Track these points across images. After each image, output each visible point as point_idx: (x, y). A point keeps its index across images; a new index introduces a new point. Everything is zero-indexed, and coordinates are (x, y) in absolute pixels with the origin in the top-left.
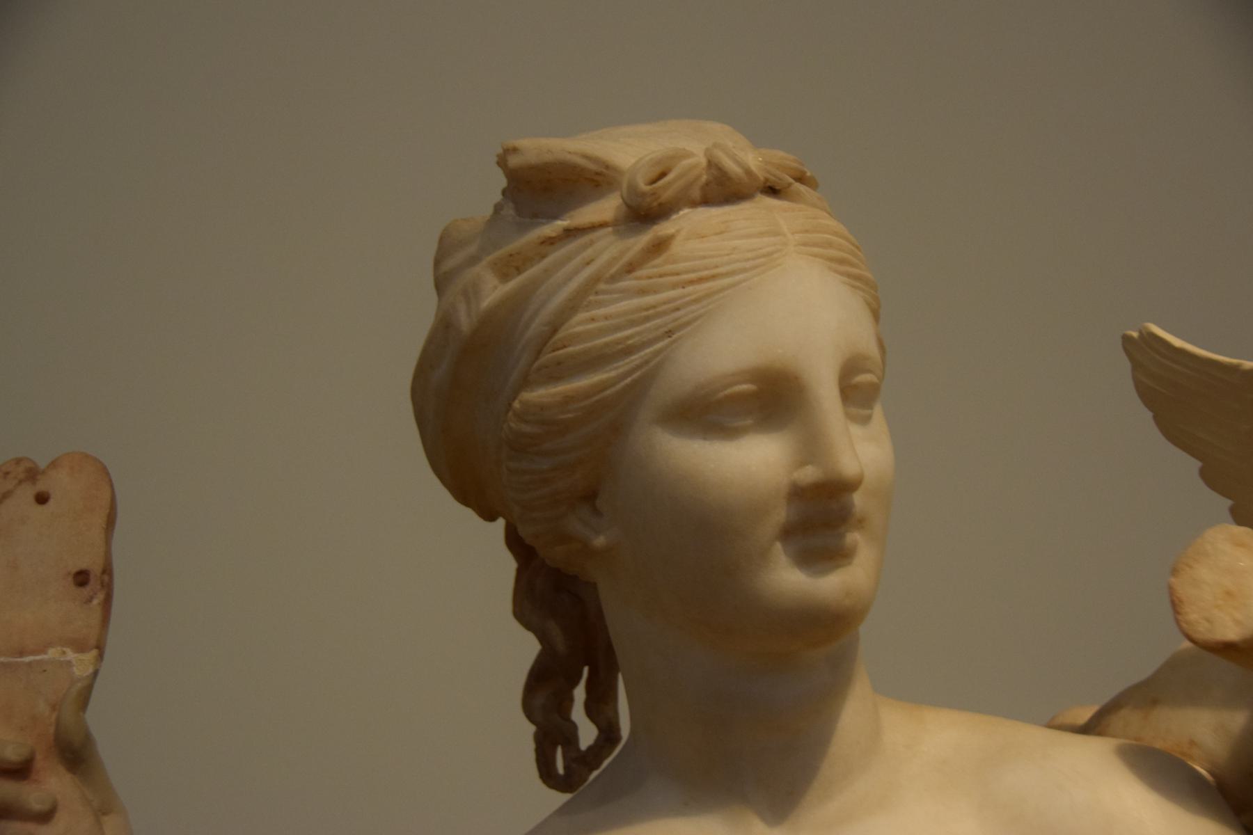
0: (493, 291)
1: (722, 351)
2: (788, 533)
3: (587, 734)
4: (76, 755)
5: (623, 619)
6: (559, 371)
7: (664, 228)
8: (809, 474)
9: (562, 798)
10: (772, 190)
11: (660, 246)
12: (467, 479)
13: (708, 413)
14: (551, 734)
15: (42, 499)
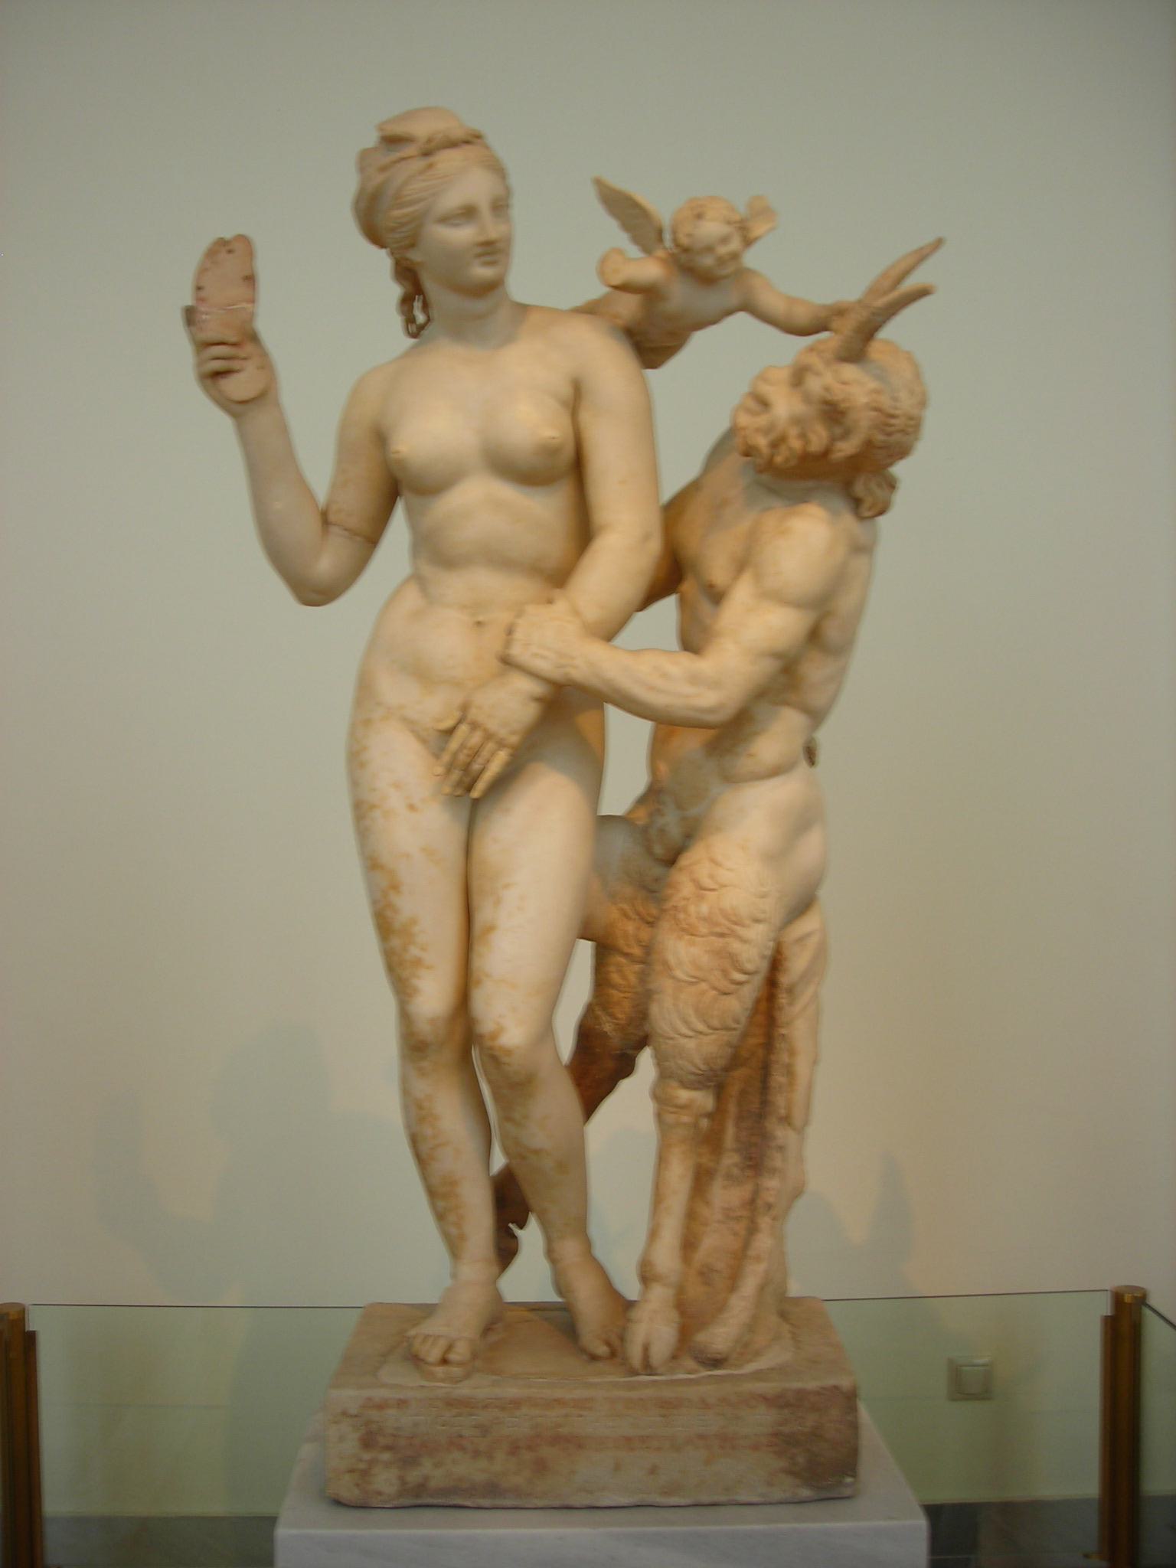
0: (380, 178)
1: (452, 200)
2: (479, 256)
3: (421, 318)
4: (254, 338)
5: (429, 285)
6: (401, 206)
7: (431, 159)
8: (482, 238)
9: (413, 341)
10: (467, 142)
11: (430, 166)
12: (374, 235)
13: (446, 219)
14: (410, 320)
15: (230, 252)
